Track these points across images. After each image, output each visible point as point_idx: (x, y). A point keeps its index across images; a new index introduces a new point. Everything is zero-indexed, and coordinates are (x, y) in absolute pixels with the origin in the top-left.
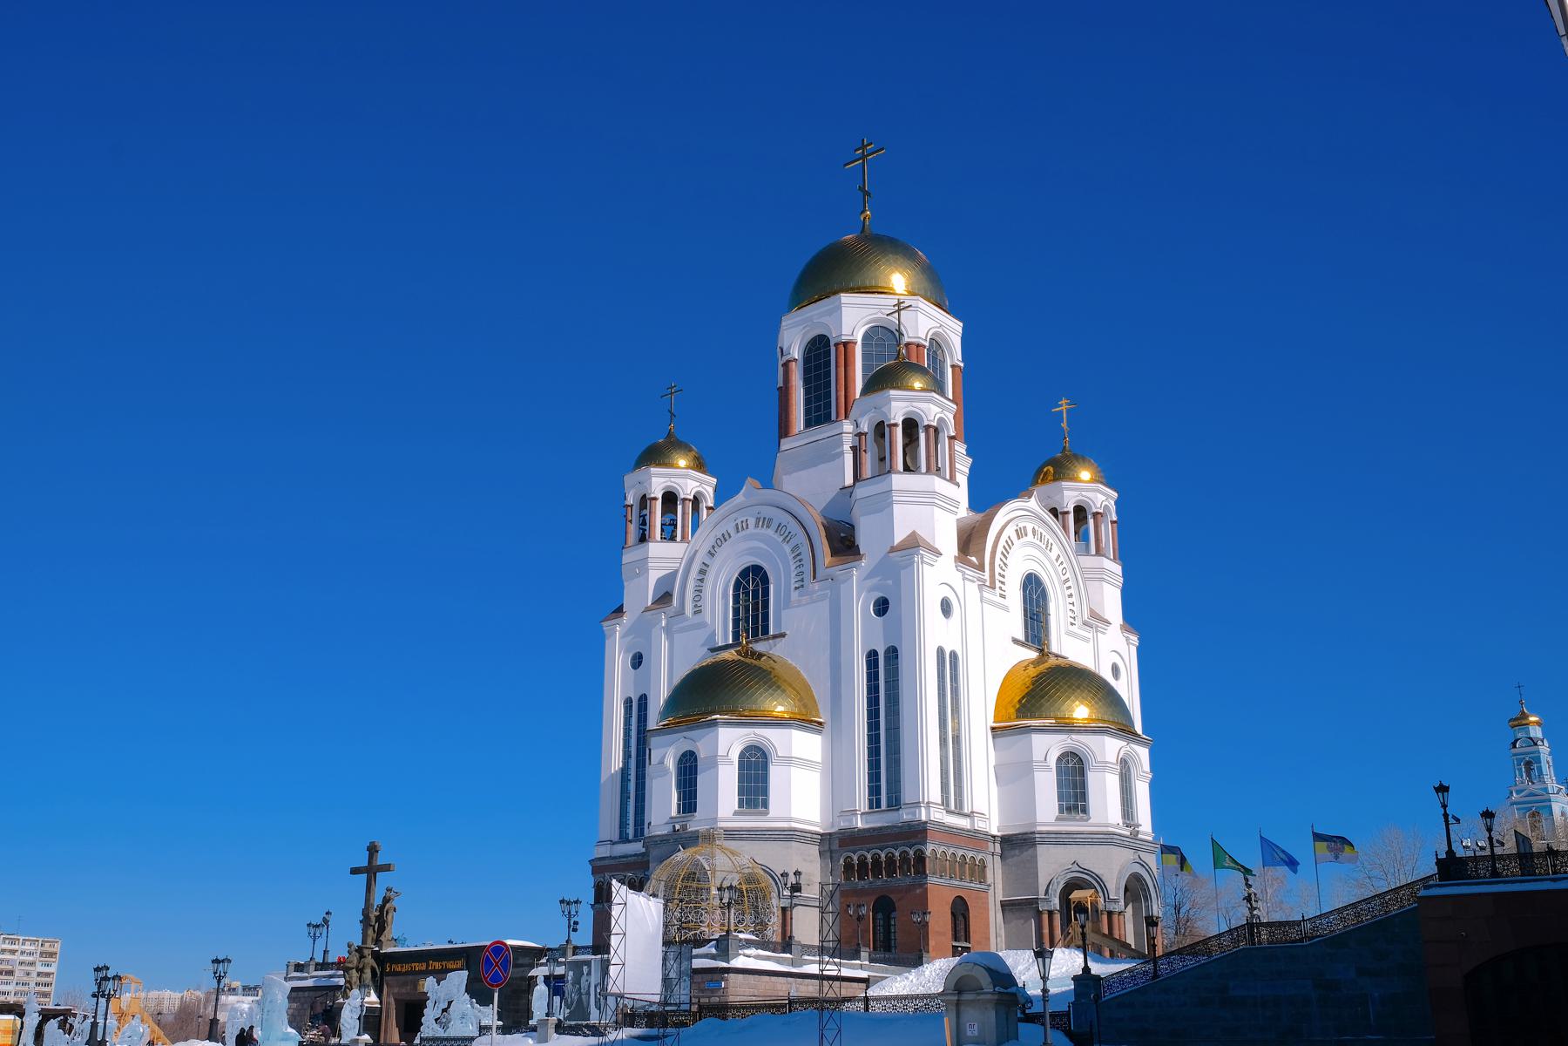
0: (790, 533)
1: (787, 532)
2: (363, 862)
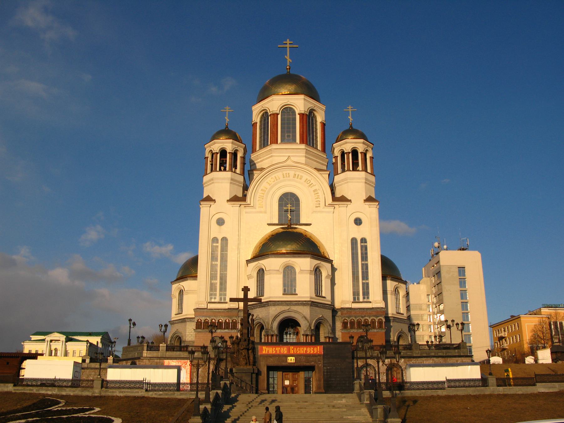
0: (312, 184)
1: (310, 183)
2: (241, 296)
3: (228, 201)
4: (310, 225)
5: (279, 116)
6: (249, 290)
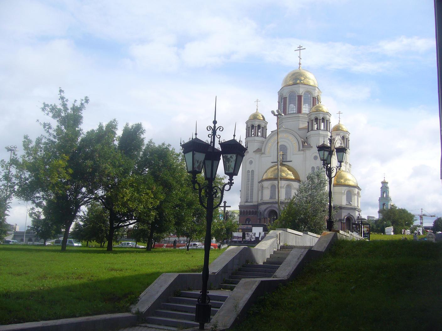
3: (254, 152)
4: (291, 161)
5: (288, 99)
6: (226, 202)
